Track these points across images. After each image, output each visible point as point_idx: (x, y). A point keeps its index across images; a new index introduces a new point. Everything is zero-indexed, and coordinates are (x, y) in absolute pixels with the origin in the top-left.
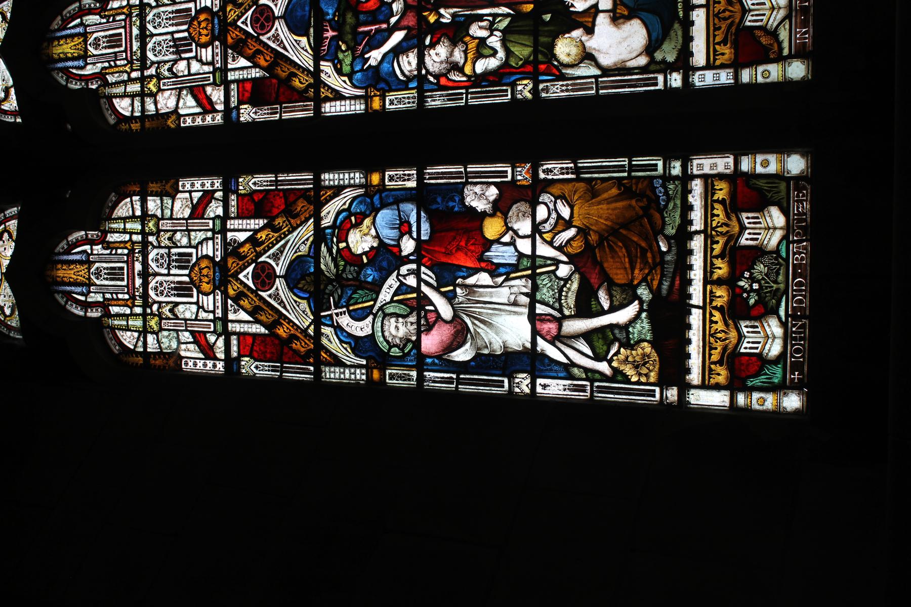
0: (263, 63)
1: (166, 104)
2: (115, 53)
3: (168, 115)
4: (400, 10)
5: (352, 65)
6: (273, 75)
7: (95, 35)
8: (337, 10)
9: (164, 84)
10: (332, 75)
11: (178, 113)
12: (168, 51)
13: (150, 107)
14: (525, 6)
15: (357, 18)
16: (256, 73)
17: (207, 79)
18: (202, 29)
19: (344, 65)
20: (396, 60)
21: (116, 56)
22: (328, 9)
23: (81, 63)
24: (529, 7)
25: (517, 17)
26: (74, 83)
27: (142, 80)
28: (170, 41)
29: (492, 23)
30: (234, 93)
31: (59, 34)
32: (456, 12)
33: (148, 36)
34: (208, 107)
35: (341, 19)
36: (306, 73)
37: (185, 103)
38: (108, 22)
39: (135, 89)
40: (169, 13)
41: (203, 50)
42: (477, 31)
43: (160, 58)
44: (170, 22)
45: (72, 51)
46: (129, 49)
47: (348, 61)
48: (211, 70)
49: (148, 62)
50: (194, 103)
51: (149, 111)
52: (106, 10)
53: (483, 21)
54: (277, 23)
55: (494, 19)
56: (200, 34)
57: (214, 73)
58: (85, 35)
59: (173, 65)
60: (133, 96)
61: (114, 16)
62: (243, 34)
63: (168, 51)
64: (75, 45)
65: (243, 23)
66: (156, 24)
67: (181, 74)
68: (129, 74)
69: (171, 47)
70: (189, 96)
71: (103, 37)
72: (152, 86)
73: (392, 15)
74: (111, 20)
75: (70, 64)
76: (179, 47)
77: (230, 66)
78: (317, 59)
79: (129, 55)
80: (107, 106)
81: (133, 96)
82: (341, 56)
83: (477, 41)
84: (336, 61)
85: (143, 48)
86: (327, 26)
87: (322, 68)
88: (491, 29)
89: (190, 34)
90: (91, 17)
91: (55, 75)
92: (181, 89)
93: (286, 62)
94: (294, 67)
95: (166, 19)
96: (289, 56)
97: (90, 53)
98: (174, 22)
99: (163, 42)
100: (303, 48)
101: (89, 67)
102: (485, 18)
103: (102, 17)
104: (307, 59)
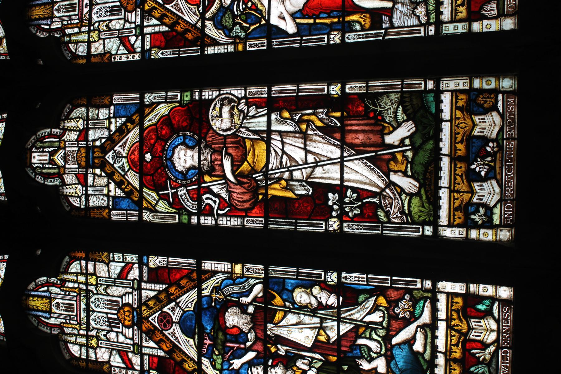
0: (165, 347)
1: (102, 356)
2: (70, 315)
3: (103, 363)
4: (252, 339)
5: (222, 364)
6: (172, 358)
7: (57, 300)
8: (213, 328)
9: (101, 343)
10: (209, 367)
11: (110, 364)
12: (104, 324)
13: (92, 356)
14: (332, 357)
15: (226, 337)
16: (160, 353)
17: (129, 348)
18: (126, 316)
19: (217, 363)
20: (249, 369)
21: (70, 317)
22: (207, 326)
23: (47, 315)
24: (334, 359)
25: (326, 363)
26: (43, 326)
27: (87, 337)
28: (105, 318)
29: (311, 363)
30: (146, 362)
31: (33, 293)
32: (288, 350)
33: (91, 311)
34: (130, 366)
35: (215, 335)
36: (192, 361)
37: (114, 359)
38: (65, 294)
39: (82, 341)
40: (105, 300)
41: (127, 330)
42: (299, 363)
43: (98, 326)
44: (106, 306)
45: (42, 307)
46: (78, 315)
47: (219, 361)
48: (132, 343)
49: (91, 327)
50: (120, 360)
51: (91, 357)
52: (64, 287)
53: (305, 359)
54: (174, 325)
55: (312, 360)
56: (125, 319)
57: (134, 345)
58: (50, 298)
59: (107, 333)
60: (81, 345)
61: (69, 292)
62: (153, 327)
63: (104, 324)
64: (43, 303)
65: (152, 319)
66: (96, 305)
67: (112, 340)
68: (78, 331)
69: (106, 321)
70: (117, 356)
71: (62, 303)
72: (93, 342)
73: (248, 341)
74: (67, 293)
75: (40, 314)
76: (112, 323)
77: (144, 344)
78: (200, 355)
79: (79, 319)
80: (64, 347)
81: (81, 345)
82: (215, 357)
83: (301, 371)
84: (212, 360)
85: (88, 317)
86: (206, 336)
87: (203, 361)
88: (310, 365)
89: (118, 317)
90: (54, 288)
91: (30, 318)
92: (112, 350)
93: (180, 352)
94: (185, 356)
95: (103, 303)
96: (182, 348)
97: (53, 311)
98: (108, 307)
99: (101, 317)
100: (191, 346)
101: (52, 319)
102: (306, 358)
103: (61, 290)
104: (193, 353)
